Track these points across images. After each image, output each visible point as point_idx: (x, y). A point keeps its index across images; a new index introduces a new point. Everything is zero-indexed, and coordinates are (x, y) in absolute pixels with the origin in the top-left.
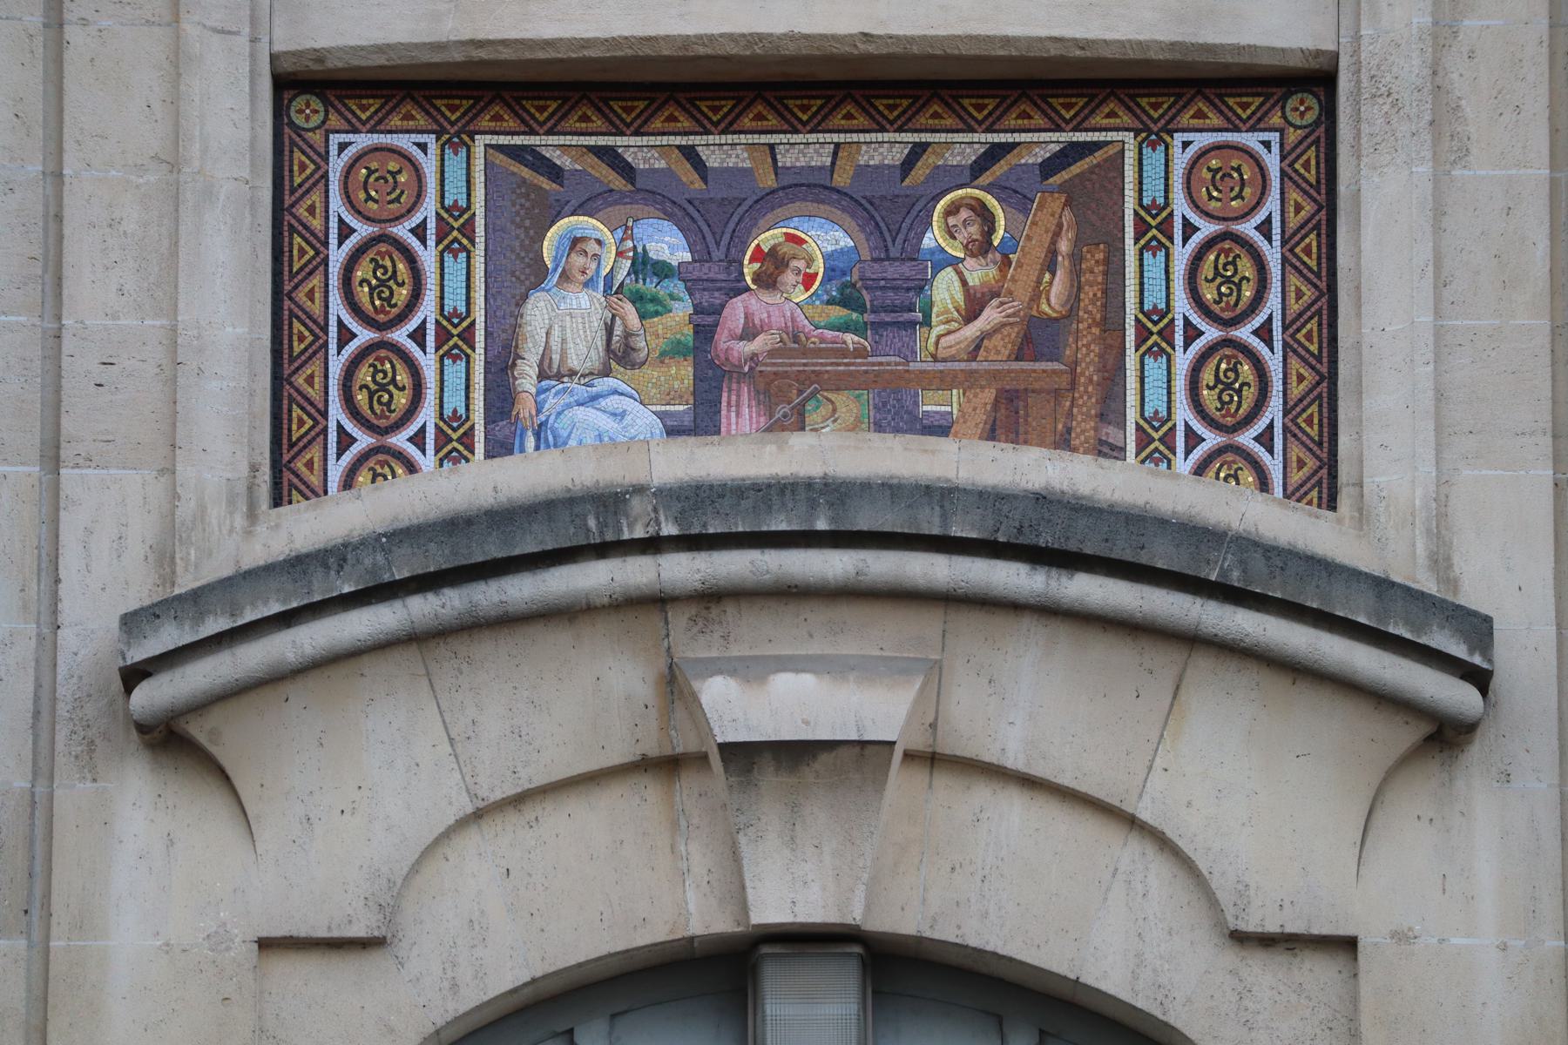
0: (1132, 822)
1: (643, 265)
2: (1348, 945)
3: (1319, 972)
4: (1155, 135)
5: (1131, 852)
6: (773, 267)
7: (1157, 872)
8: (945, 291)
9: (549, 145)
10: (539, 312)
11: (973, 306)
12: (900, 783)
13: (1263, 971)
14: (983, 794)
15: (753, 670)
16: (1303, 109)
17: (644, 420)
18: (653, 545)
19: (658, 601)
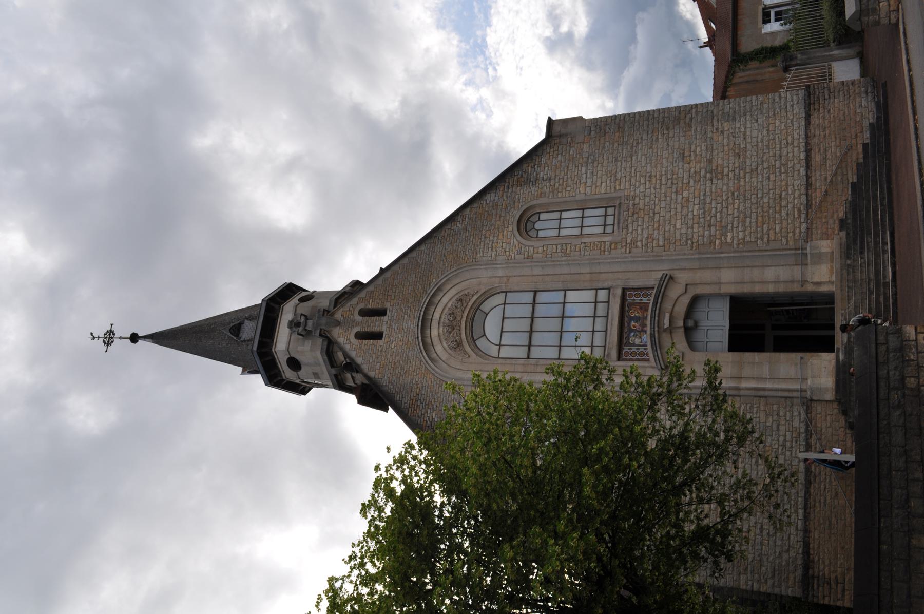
0: (677, 300)
1: (634, 336)
2: (687, 285)
3: (688, 287)
4: (627, 300)
5: (679, 300)
6: (634, 327)
7: (681, 298)
8: (637, 315)
9: (624, 342)
10: (637, 343)
11: (638, 313)
12: (674, 314)
13: (689, 290)
14: (675, 310)
15: (664, 324)
16: (626, 290)
17: (645, 336)
18: (654, 331)
19: (658, 331)
